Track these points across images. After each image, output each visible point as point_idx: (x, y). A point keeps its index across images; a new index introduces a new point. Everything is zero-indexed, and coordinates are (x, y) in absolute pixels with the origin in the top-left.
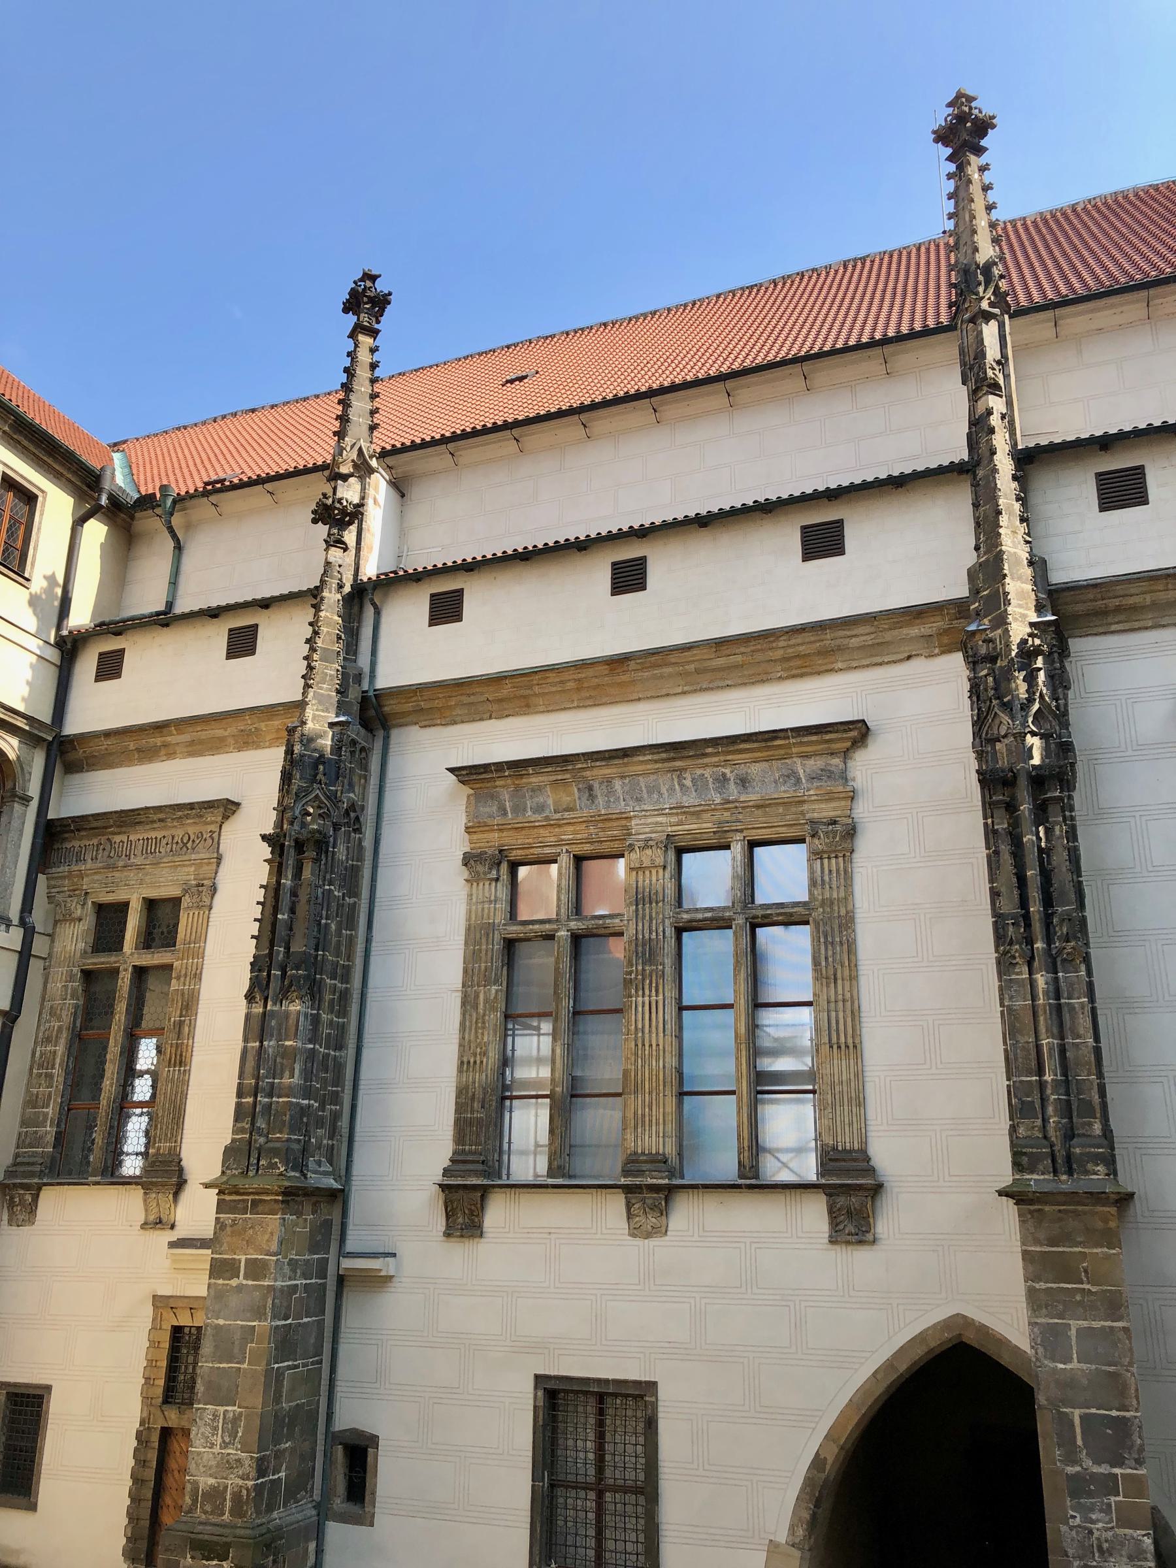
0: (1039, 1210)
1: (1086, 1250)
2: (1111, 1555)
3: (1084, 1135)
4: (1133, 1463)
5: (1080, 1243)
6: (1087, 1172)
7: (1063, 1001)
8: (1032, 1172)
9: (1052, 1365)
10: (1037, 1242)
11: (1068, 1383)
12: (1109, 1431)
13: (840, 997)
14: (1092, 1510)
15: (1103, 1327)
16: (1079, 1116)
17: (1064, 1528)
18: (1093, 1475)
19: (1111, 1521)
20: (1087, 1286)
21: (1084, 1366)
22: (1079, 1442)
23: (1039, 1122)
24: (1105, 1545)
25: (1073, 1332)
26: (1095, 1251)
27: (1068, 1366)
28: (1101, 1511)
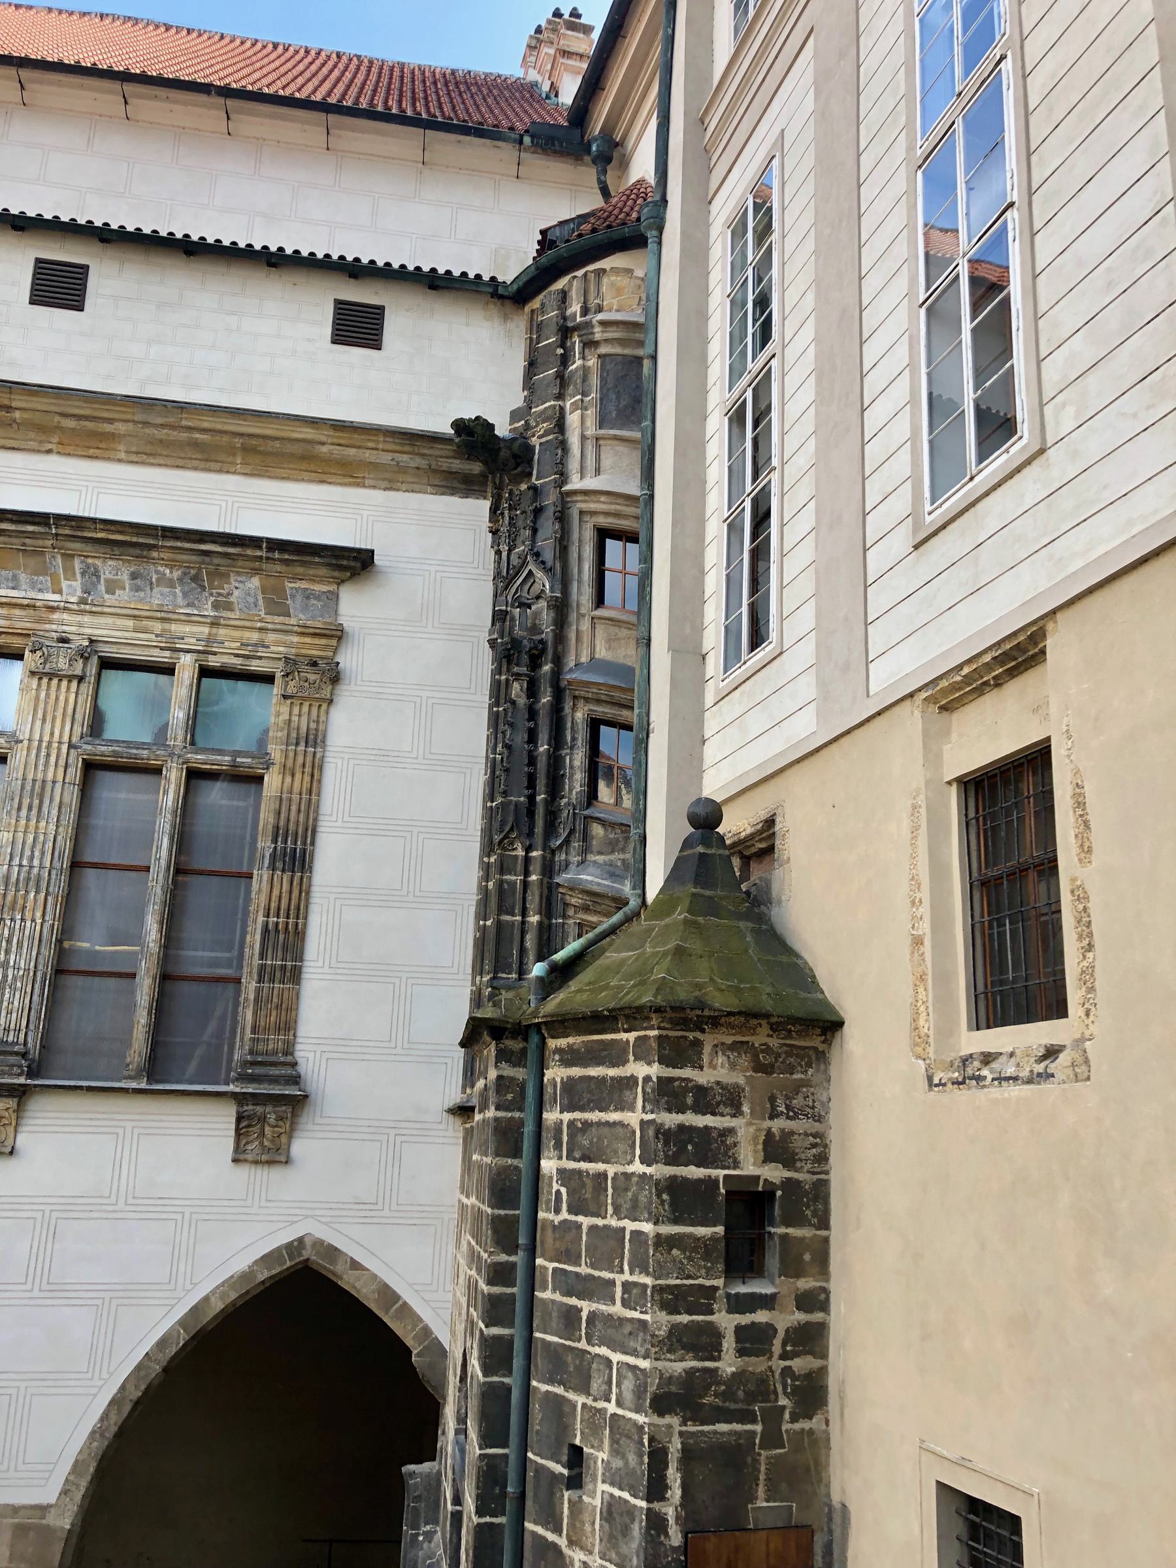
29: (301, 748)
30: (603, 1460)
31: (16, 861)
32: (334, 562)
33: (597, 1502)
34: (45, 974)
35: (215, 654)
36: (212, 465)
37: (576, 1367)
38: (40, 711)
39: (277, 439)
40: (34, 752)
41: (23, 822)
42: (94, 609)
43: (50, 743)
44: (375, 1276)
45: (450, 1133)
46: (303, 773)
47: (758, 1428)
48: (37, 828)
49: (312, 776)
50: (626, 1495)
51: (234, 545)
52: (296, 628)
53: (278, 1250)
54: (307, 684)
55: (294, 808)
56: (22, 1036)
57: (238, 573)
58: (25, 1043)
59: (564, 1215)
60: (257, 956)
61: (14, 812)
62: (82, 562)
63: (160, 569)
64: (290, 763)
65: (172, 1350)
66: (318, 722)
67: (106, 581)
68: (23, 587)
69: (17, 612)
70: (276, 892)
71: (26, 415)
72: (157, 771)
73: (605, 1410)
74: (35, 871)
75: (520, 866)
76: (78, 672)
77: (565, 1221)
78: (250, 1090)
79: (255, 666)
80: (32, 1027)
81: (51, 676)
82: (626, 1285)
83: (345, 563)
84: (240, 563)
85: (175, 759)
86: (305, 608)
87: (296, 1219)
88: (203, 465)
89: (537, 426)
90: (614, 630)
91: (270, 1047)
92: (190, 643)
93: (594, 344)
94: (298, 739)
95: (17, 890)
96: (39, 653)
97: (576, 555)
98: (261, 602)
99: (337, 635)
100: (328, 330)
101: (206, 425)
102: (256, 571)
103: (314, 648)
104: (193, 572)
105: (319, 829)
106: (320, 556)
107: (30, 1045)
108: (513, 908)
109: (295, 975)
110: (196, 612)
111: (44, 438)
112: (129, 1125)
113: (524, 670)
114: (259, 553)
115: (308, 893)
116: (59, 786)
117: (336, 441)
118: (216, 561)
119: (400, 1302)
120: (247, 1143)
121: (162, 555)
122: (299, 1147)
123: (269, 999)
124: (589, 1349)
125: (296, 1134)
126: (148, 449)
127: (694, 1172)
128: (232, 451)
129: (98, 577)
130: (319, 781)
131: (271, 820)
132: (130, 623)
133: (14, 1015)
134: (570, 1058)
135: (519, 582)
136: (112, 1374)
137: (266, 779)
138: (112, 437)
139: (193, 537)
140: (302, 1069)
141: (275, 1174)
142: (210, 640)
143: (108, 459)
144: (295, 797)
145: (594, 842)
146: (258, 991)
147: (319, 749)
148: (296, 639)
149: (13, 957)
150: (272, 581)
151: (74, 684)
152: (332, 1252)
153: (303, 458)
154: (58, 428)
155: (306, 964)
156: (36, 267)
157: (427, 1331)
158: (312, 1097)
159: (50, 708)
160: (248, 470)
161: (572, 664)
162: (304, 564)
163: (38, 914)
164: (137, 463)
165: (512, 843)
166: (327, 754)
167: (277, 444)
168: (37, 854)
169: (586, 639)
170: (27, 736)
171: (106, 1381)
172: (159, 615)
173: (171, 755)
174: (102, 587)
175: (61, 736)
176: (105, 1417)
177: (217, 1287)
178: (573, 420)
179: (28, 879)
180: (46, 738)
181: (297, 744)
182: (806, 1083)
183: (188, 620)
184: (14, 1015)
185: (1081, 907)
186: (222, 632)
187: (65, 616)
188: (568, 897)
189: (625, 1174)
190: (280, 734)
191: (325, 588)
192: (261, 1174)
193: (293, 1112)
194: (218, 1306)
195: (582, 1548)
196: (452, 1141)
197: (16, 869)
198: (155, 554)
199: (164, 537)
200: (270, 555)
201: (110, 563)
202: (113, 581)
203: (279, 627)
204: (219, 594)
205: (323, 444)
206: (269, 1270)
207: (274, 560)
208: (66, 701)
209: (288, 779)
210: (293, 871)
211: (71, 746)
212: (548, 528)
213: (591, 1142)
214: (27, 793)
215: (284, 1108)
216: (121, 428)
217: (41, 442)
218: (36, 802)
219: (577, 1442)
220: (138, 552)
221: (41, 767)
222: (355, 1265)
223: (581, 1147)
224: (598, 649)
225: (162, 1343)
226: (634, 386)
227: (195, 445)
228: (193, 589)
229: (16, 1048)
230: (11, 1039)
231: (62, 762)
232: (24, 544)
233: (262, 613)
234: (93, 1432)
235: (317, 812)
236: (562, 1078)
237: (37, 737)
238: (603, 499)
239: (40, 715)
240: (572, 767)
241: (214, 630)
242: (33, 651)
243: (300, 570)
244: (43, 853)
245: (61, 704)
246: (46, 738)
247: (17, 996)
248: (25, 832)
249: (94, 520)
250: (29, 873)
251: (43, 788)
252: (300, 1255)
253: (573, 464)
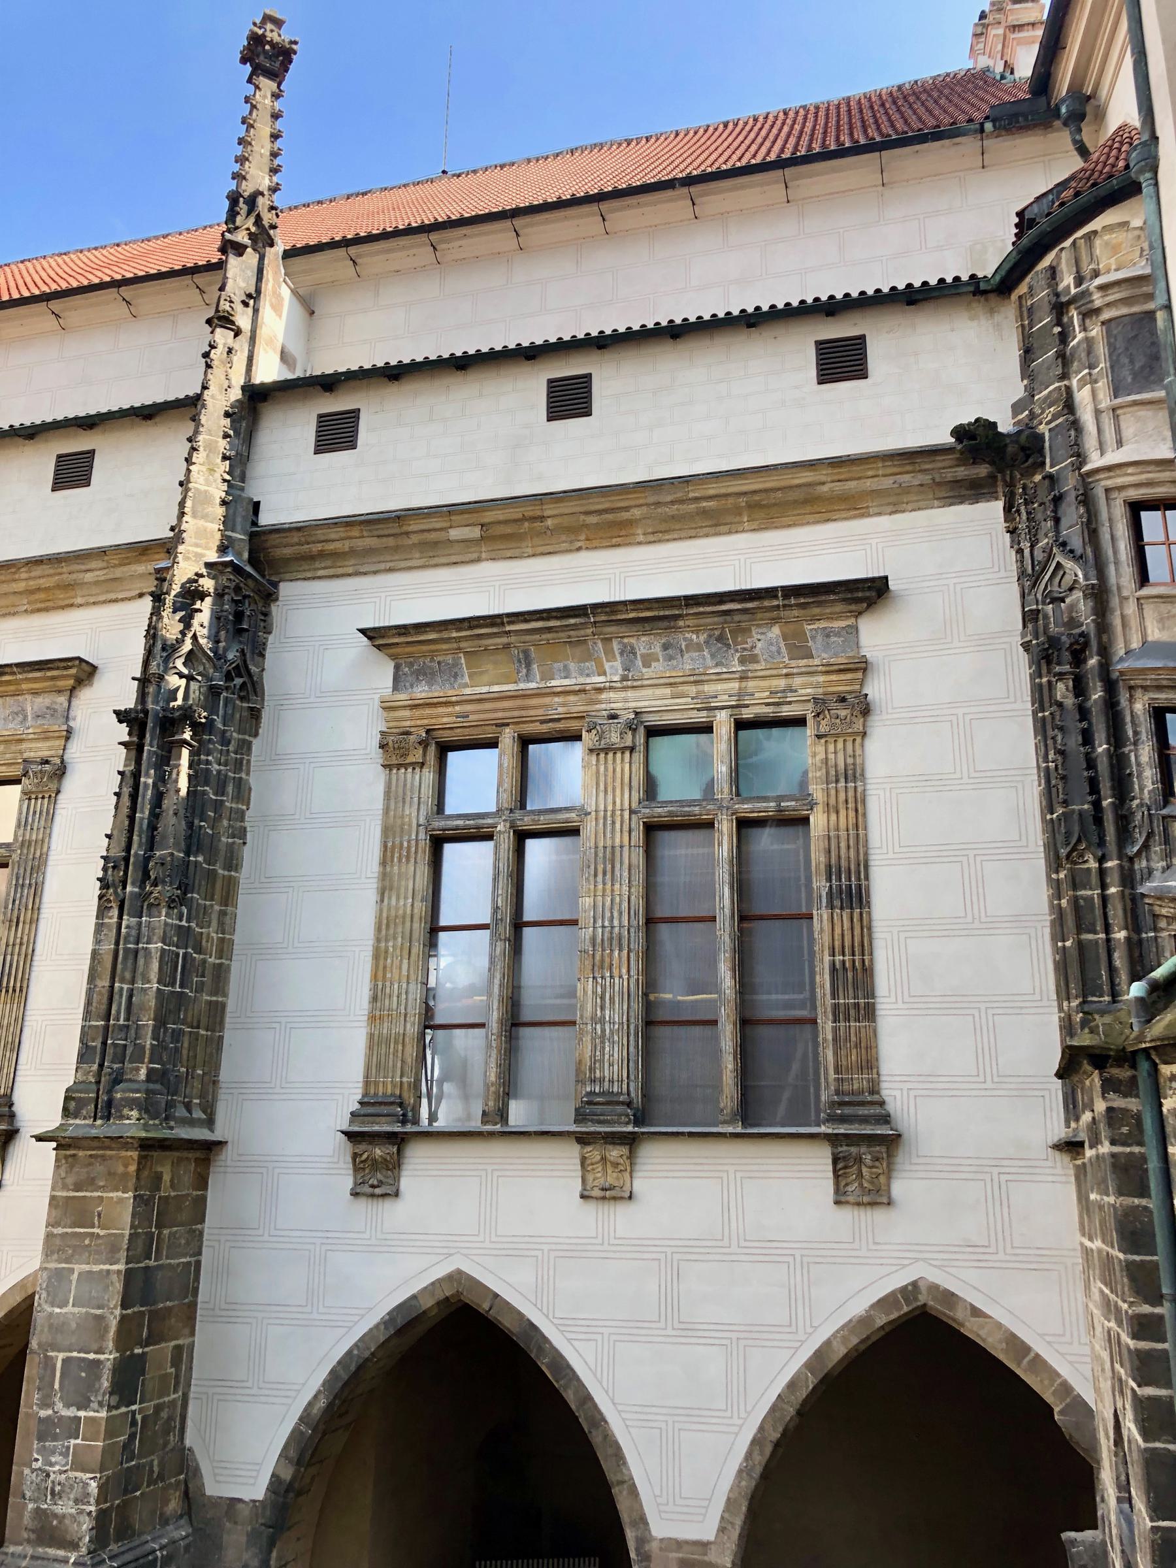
0: (74, 1155)
1: (105, 1195)
2: (60, 1498)
3: (130, 1080)
4: (95, 1405)
5: (100, 1187)
6: (122, 1117)
7: (141, 945)
8: (76, 1117)
9: (49, 1309)
10: (65, 1187)
11: (58, 1327)
12: (83, 1374)
13: (18, 941)
14: (53, 1453)
15: (101, 1271)
16: (131, 1062)
17: (27, 1471)
18: (61, 1418)
19: (67, 1464)
20: (96, 1230)
21: (76, 1310)
22: (57, 1386)
23: (95, 1067)
24: (58, 1488)
25: (75, 1276)
26: (111, 1195)
27: (64, 1310)
28: (61, 1454)
29: (842, 784)
31: (599, 923)
32: (849, 596)
34: (637, 1027)
35: (747, 706)
36: (718, 528)
38: (601, 784)
39: (779, 489)
40: (601, 821)
41: (600, 887)
42: (635, 684)
43: (613, 811)
45: (1059, 1171)
46: (847, 809)
48: (613, 890)
49: (857, 811)
51: (751, 599)
52: (820, 668)
53: (893, 1294)
54: (838, 721)
55: (843, 845)
56: (625, 1086)
57: (759, 626)
58: (629, 1093)
60: (828, 996)
61: (592, 878)
62: (620, 643)
63: (687, 635)
64: (832, 801)
65: (803, 1393)
66: (854, 756)
67: (642, 656)
68: (574, 675)
69: (572, 698)
70: (838, 931)
71: (556, 521)
72: (710, 825)
74: (616, 930)
75: (1094, 879)
76: (629, 743)
78: (842, 1131)
79: (786, 711)
80: (632, 1077)
81: (606, 750)
83: (860, 594)
84: (759, 616)
85: (725, 811)
86: (827, 647)
87: (906, 1262)
88: (712, 530)
89: (1042, 413)
90: (1165, 608)
91: (856, 1087)
92: (723, 700)
93: (1097, 311)
94: (837, 776)
95: (603, 950)
96: (594, 732)
97: (1108, 536)
98: (784, 650)
99: (862, 667)
100: (813, 373)
101: (712, 492)
102: (775, 621)
103: (841, 684)
104: (717, 633)
105: (871, 863)
106: (835, 593)
107: (633, 1095)
108: (1094, 925)
109: (869, 1012)
110: (725, 670)
111: (573, 537)
112: (731, 1169)
113: (1067, 668)
114: (775, 603)
115: (870, 928)
116: (626, 849)
117: (836, 478)
118: (737, 618)
119: (1032, 1355)
120: (847, 1185)
121: (688, 623)
122: (899, 1188)
123: (848, 1039)
125: (895, 1174)
126: (663, 527)
128: (738, 511)
129: (635, 654)
130: (864, 815)
131: (822, 859)
132: (668, 691)
133: (616, 1067)
135: (1047, 577)
136: (749, 1413)
137: (812, 819)
138: (630, 523)
139: (713, 600)
140: (891, 1107)
141: (879, 1216)
142: (740, 694)
143: (629, 544)
144: (843, 834)
146: (835, 1030)
147: (859, 783)
148: (821, 678)
149: (607, 1012)
150: (792, 627)
151: (627, 754)
152: (949, 1297)
153: (806, 502)
154: (587, 526)
155: (878, 1000)
156: (549, 387)
157: (1066, 1388)
158: (905, 1136)
159: (610, 780)
160: (755, 525)
161: (1122, 652)
162: (819, 604)
163: (624, 971)
164: (654, 542)
165: (1082, 856)
166: (868, 787)
167: (779, 494)
168: (616, 914)
169: (1134, 623)
170: (594, 808)
171: (745, 1419)
172: (692, 679)
173: (720, 808)
174: (639, 663)
175: (622, 804)
176: (749, 1455)
177: (837, 1331)
178: (1082, 396)
179: (611, 939)
180: (610, 808)
181: (837, 781)
183: (719, 678)
184: (616, 1067)
186: (751, 684)
187: (612, 695)
188: (1156, 908)
190: (818, 774)
191: (843, 624)
192: (866, 1216)
193: (888, 1152)
194: (840, 1351)
196: (1063, 1179)
197: (600, 930)
198: (681, 623)
199: (686, 605)
200: (786, 602)
201: (643, 639)
202: (649, 655)
203: (803, 670)
204: (745, 649)
205: (823, 483)
206: (887, 1315)
207: (791, 606)
208: (622, 770)
209: (833, 817)
210: (852, 908)
211: (632, 812)
212: (1072, 514)
214: (600, 860)
215: (878, 1148)
216: (637, 513)
217: (571, 542)
218: (609, 867)
220: (665, 624)
221: (609, 835)
222: (976, 1312)
224: (1149, 631)
225: (792, 1385)
226: (1148, 343)
227: (704, 513)
228: (720, 649)
229: (621, 1098)
230: (615, 1090)
231: (626, 828)
232: (569, 637)
233: (786, 660)
234: (740, 1471)
235: (866, 845)
237: (602, 807)
238: (1130, 470)
239: (602, 787)
240: (1138, 764)
241: (744, 684)
242: (589, 731)
243: (816, 611)
244: (621, 913)
245: (619, 775)
246: (610, 808)
247: (616, 1049)
248: (603, 896)
249: (624, 603)
250: (611, 933)
251: (613, 853)
252: (916, 1299)
253: (1090, 442)
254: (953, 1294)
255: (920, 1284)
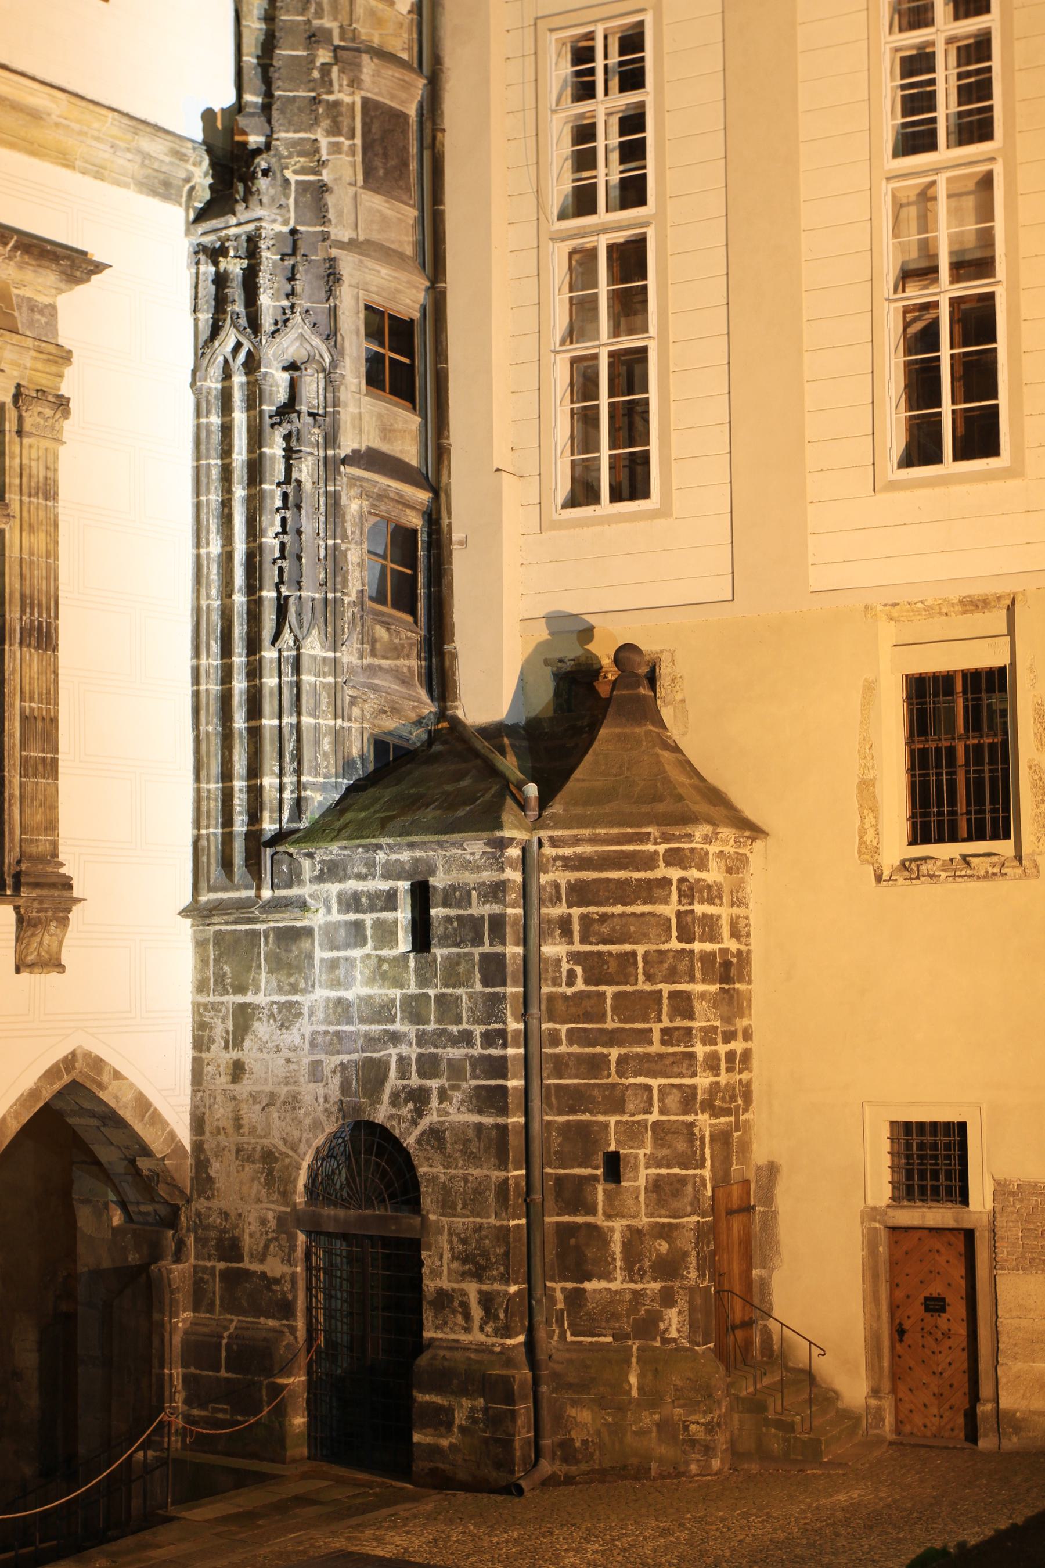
30: (645, 1154)
33: (642, 1182)
37: (604, 1097)
44: (132, 1085)
47: (732, 1119)
50: (676, 1170)
53: (57, 1064)
59: (580, 986)
73: (646, 1120)
77: (582, 991)
82: (664, 1031)
109: (51, 768)
119: (152, 1109)
124: (624, 1081)
127: (708, 947)
134: (569, 863)
145: (378, 646)
152: (98, 1063)
157: (172, 1135)
177: (11, 1107)
182: (742, 881)
185: (1036, 777)
189: (660, 952)
195: (623, 1217)
213: (613, 929)
219: (612, 1148)
222: (117, 1075)
223: (595, 933)
235: (56, 579)
236: (569, 881)
252: (74, 1068)
254: (101, 1060)
255: (78, 1052)
